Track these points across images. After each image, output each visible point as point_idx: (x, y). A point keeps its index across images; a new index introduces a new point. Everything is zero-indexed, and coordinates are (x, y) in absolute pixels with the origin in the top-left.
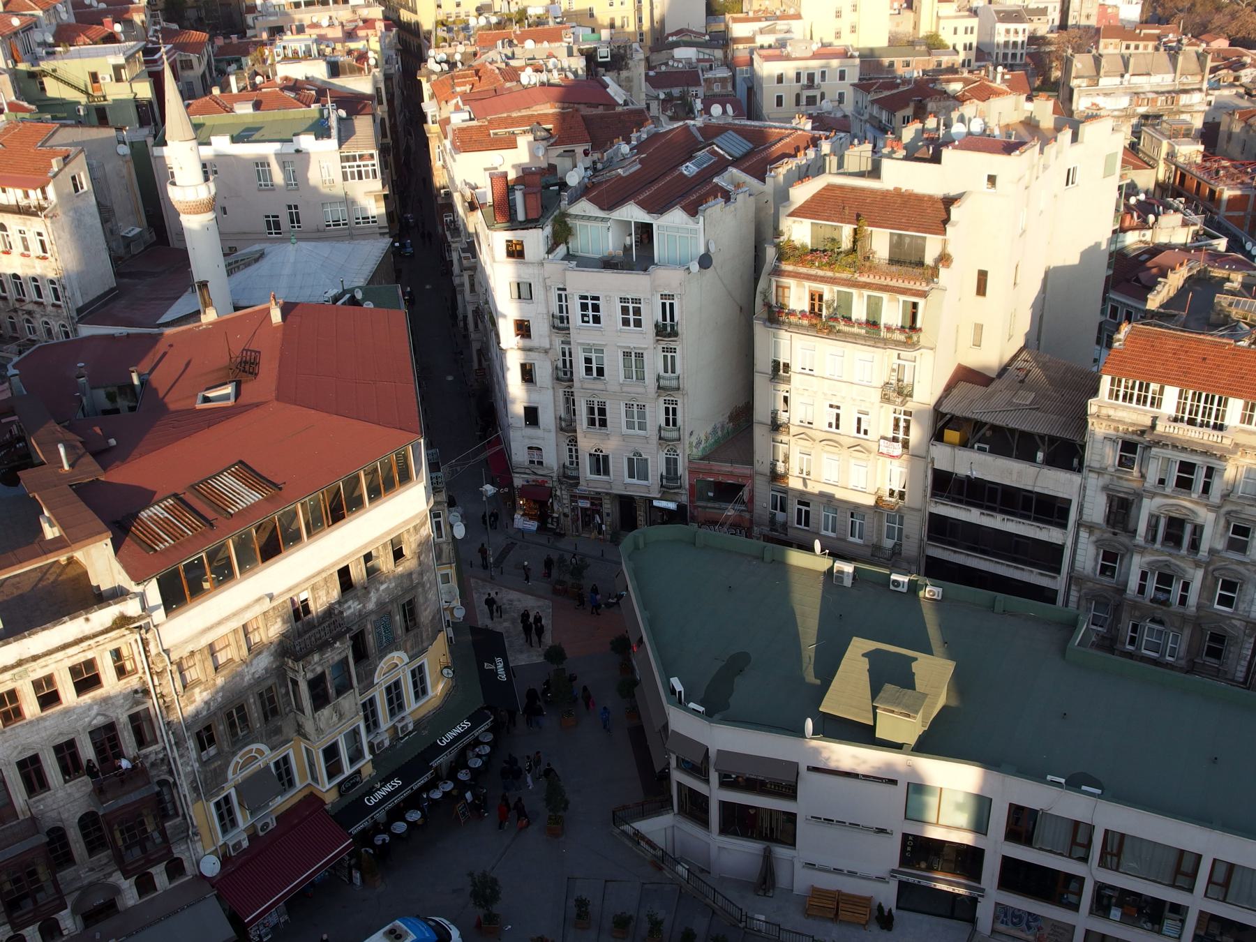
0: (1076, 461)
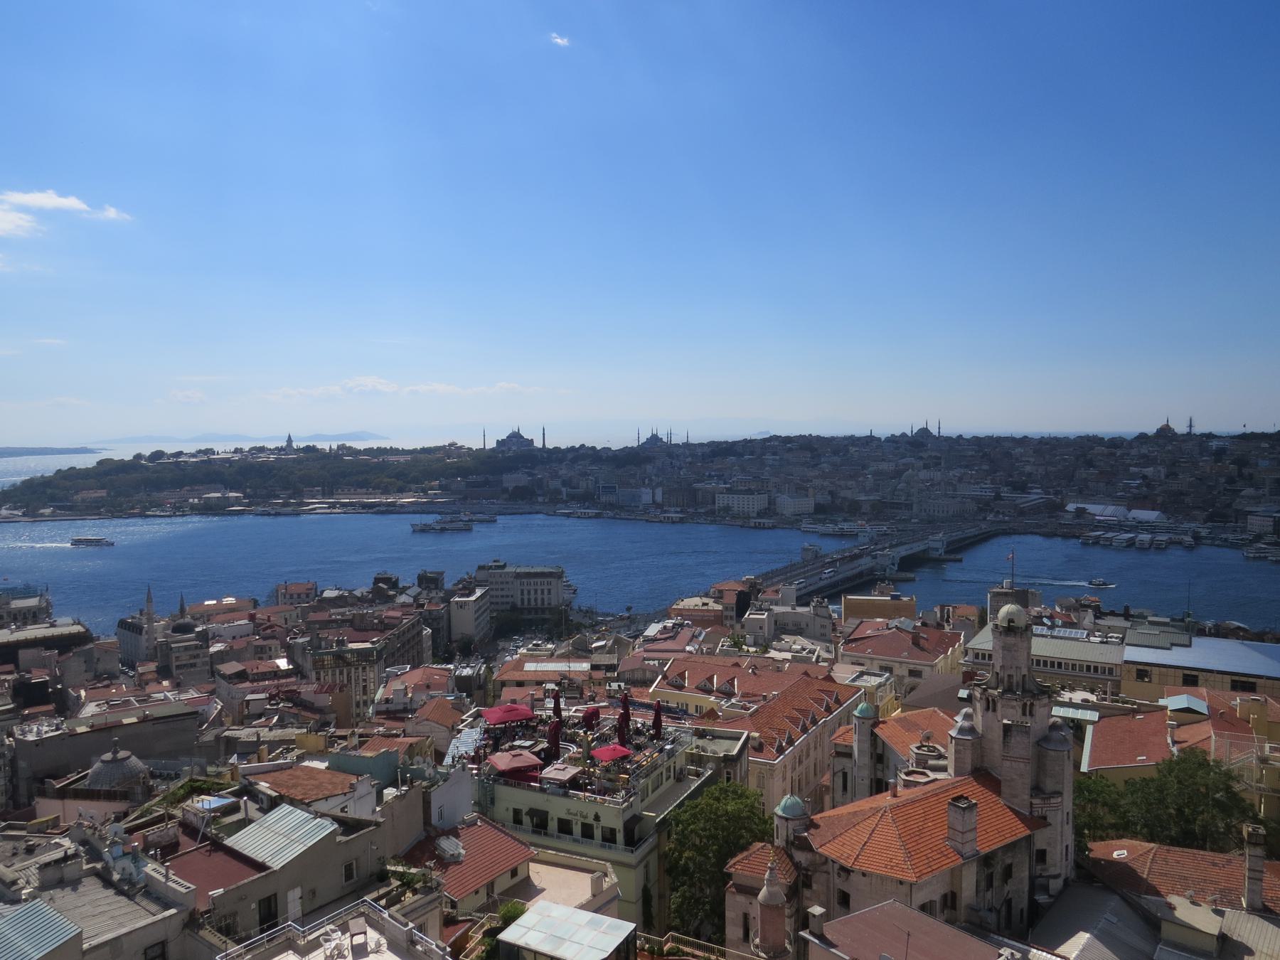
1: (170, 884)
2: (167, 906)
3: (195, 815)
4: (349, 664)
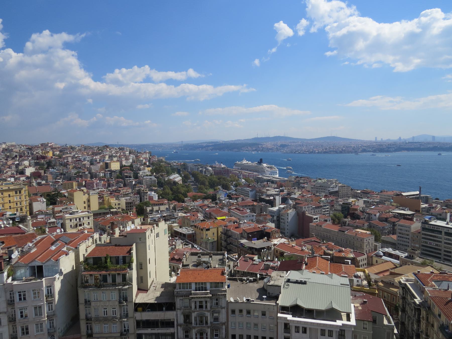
0: (173, 308)
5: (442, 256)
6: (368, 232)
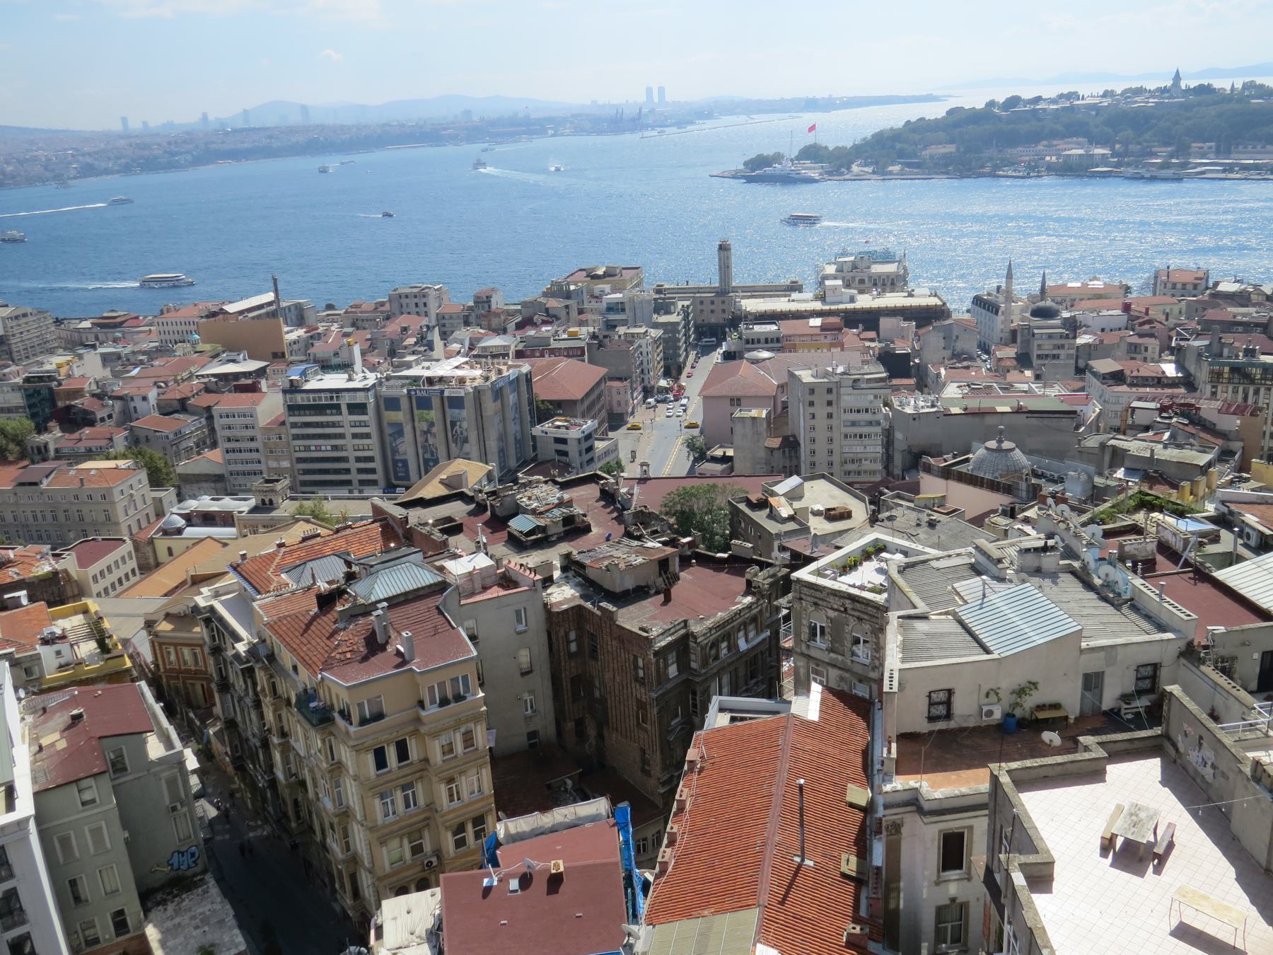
1: (1166, 605)
2: (1162, 628)
3: (1175, 534)
4: (1252, 381)
5: (355, 477)
6: (122, 463)
